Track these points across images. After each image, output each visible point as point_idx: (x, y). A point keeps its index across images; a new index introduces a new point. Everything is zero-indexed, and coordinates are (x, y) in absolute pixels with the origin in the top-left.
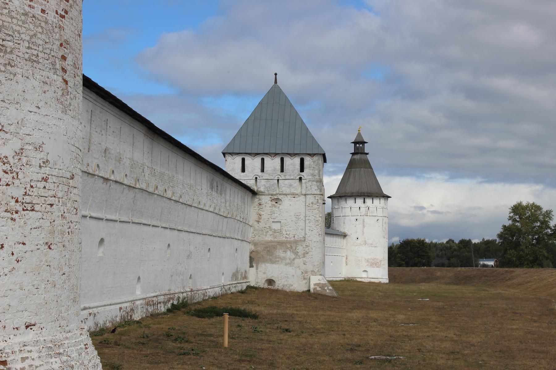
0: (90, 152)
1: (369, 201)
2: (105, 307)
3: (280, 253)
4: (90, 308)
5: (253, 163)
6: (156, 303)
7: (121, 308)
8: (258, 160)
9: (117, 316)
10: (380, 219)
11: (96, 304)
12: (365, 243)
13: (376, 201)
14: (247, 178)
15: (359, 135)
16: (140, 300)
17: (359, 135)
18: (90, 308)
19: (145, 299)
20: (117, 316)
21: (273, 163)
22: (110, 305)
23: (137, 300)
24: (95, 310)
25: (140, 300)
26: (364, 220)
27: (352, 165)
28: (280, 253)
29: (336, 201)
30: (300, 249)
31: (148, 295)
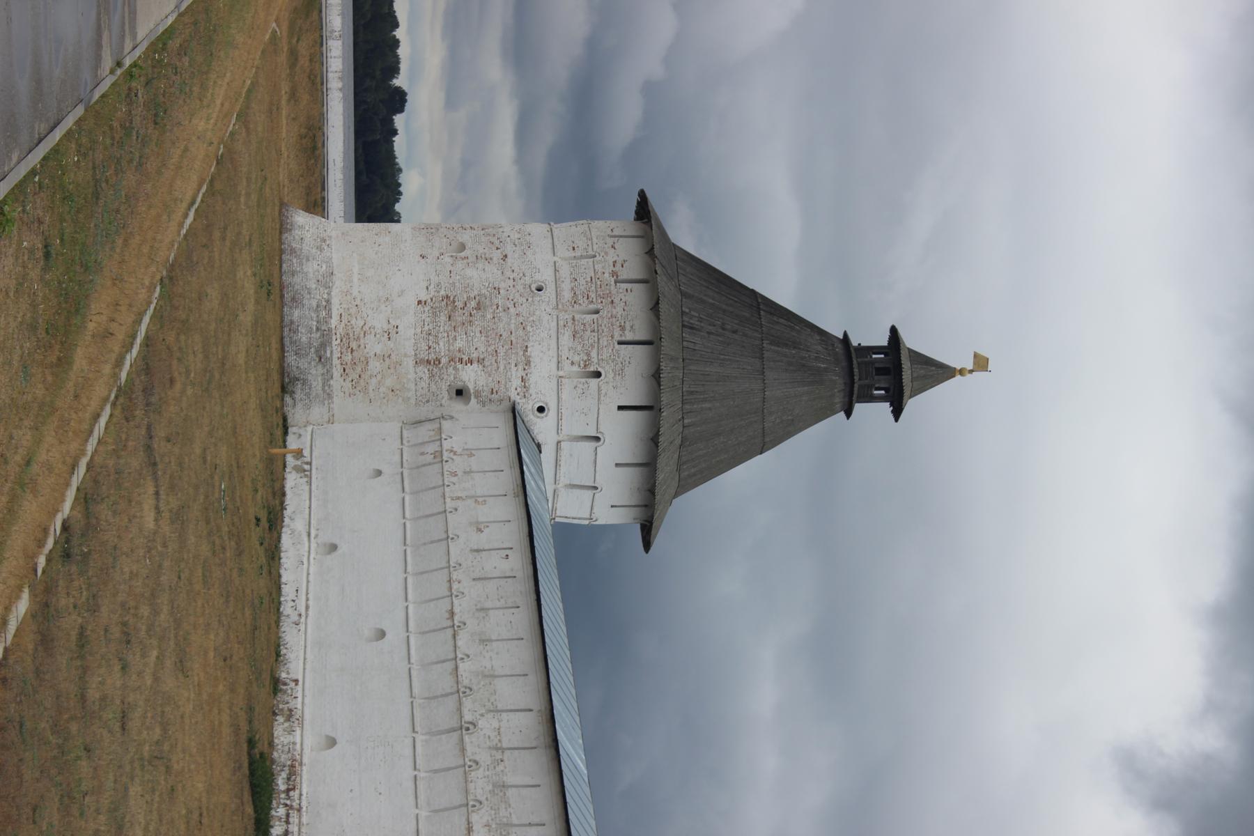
0: (474, 583)
2: (303, 648)
4: (307, 617)
6: (288, 802)
7: (296, 681)
9: (288, 673)
11: (309, 630)
16: (302, 744)
18: (307, 617)
19: (301, 764)
20: (288, 673)
22: (305, 659)
23: (302, 732)
24: (302, 627)
25: (302, 744)
31: (304, 786)
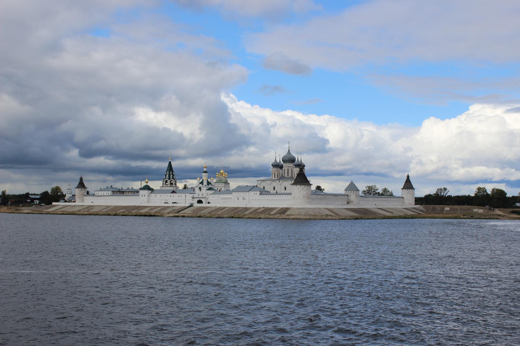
1: (409, 190)
3: (351, 202)
5: (348, 192)
8: (348, 191)
10: (412, 195)
12: (408, 199)
13: (410, 190)
14: (347, 193)
15: (408, 174)
17: (408, 174)
21: (350, 192)
26: (407, 195)
27: (406, 182)
28: (351, 202)
29: (403, 190)
30: (353, 202)
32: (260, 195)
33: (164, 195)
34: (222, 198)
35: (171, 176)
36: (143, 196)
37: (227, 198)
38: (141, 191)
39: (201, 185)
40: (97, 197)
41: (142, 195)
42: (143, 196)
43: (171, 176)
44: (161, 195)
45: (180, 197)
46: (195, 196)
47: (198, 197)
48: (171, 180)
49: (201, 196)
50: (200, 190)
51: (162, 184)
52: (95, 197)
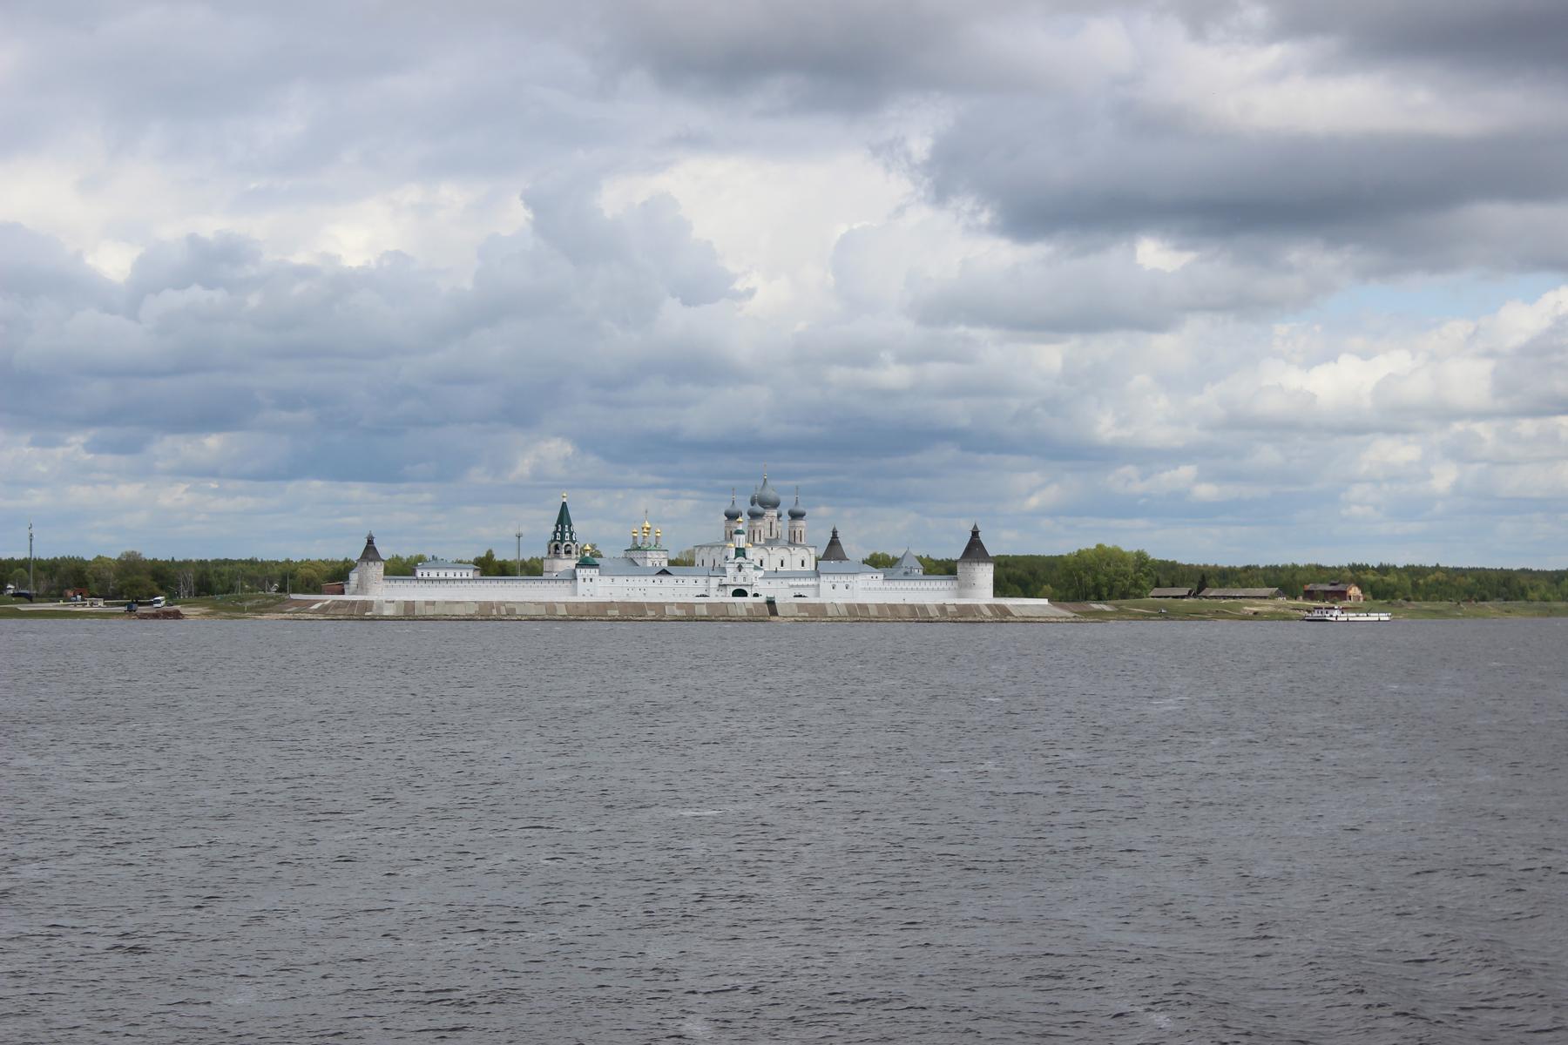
32: (886, 583)
33: (637, 578)
34: (792, 586)
35: (567, 534)
36: (588, 581)
37: (803, 586)
38: (583, 570)
39: (740, 560)
40: (422, 583)
41: (584, 580)
42: (588, 581)
43: (567, 534)
44: (631, 579)
45: (680, 582)
46: (725, 581)
47: (734, 583)
48: (568, 543)
49: (740, 581)
50: (740, 571)
51: (547, 552)
52: (415, 583)
